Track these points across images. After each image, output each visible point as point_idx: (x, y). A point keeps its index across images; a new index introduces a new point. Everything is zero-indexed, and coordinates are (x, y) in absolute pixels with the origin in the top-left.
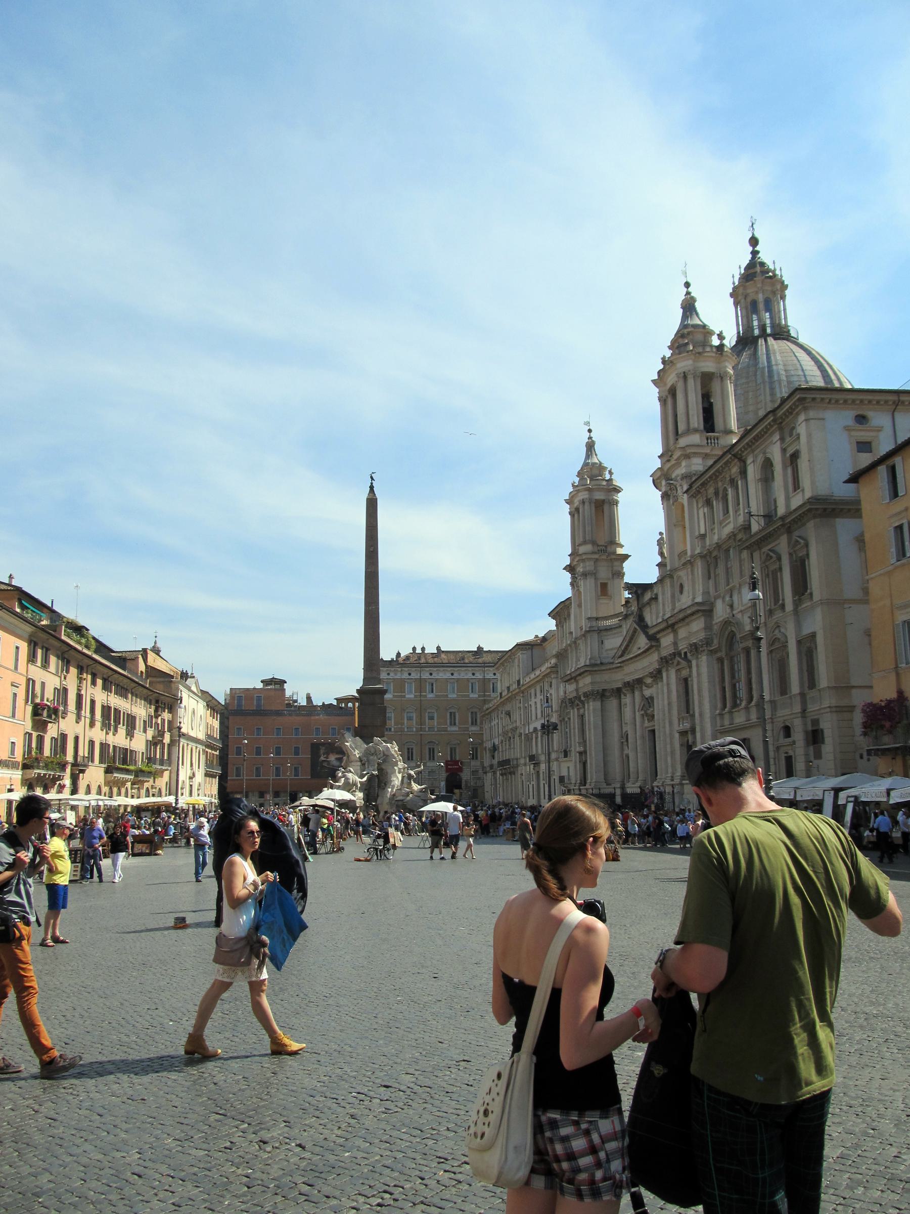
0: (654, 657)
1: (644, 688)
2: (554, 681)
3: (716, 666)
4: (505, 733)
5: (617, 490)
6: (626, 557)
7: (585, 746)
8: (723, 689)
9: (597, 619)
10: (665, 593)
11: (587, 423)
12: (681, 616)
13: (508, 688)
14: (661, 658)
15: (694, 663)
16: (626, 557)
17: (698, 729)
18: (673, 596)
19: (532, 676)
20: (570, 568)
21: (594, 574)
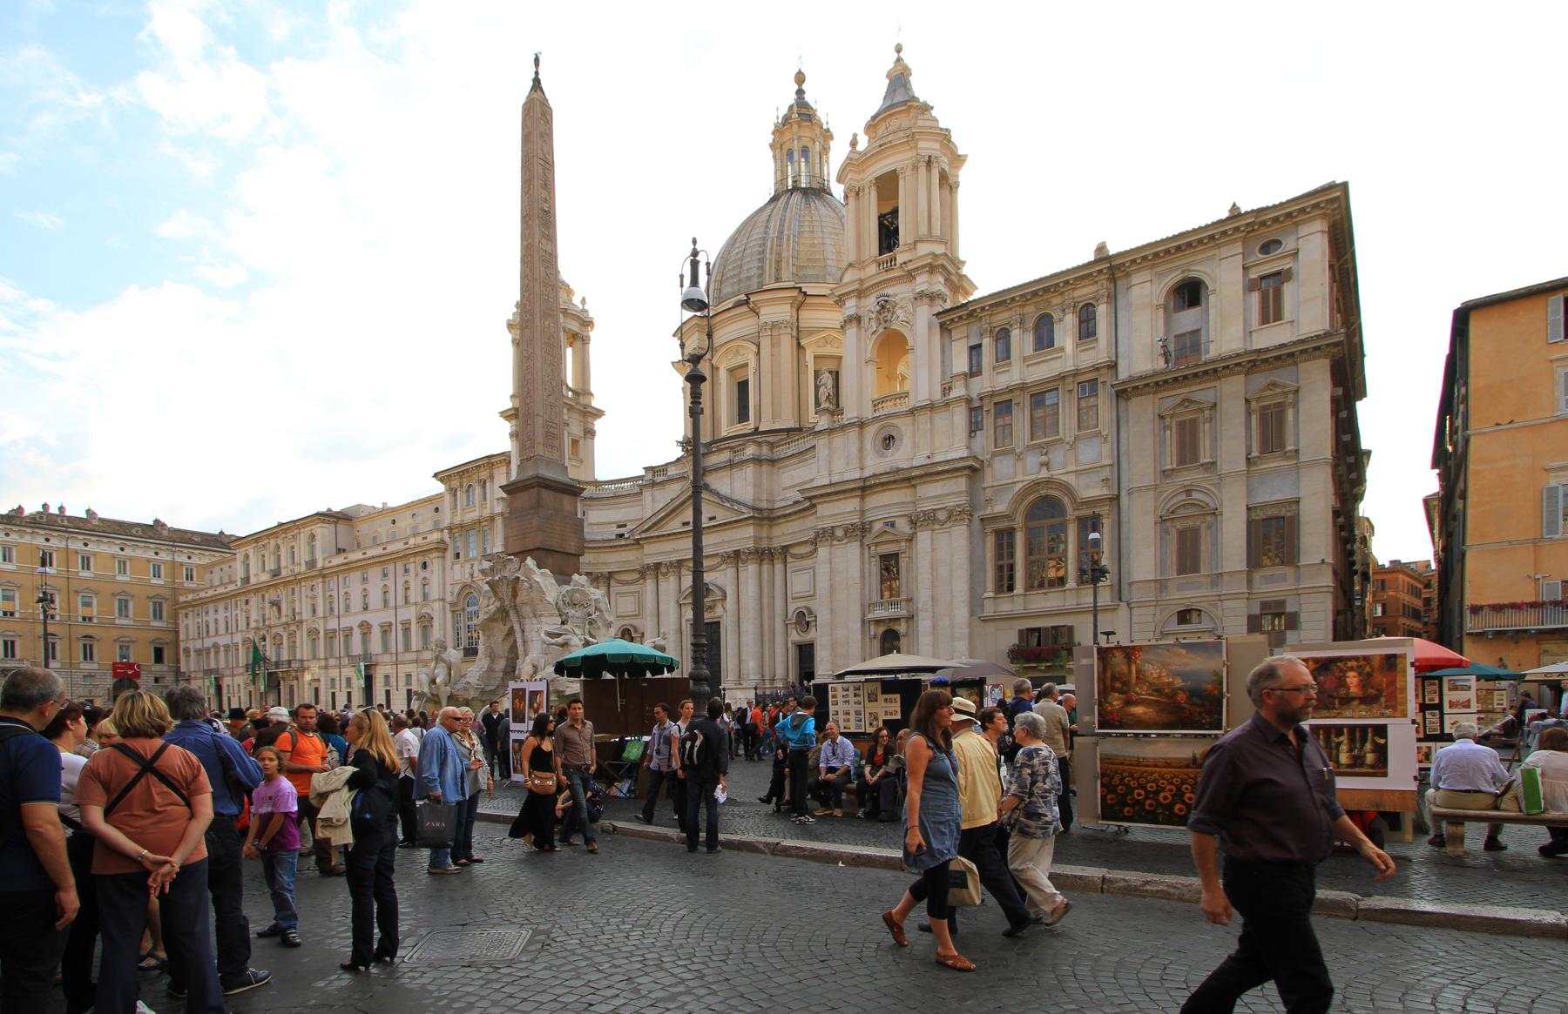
16: (599, 414)
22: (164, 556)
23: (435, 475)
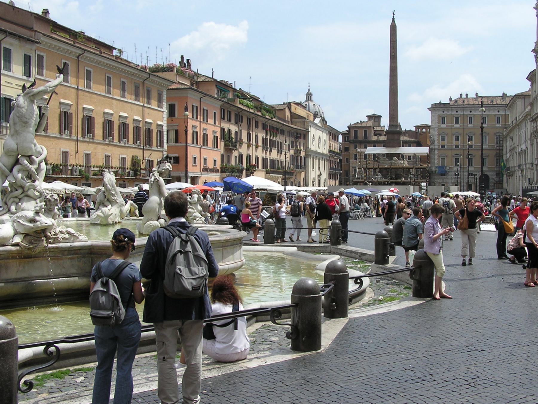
4: (511, 150)
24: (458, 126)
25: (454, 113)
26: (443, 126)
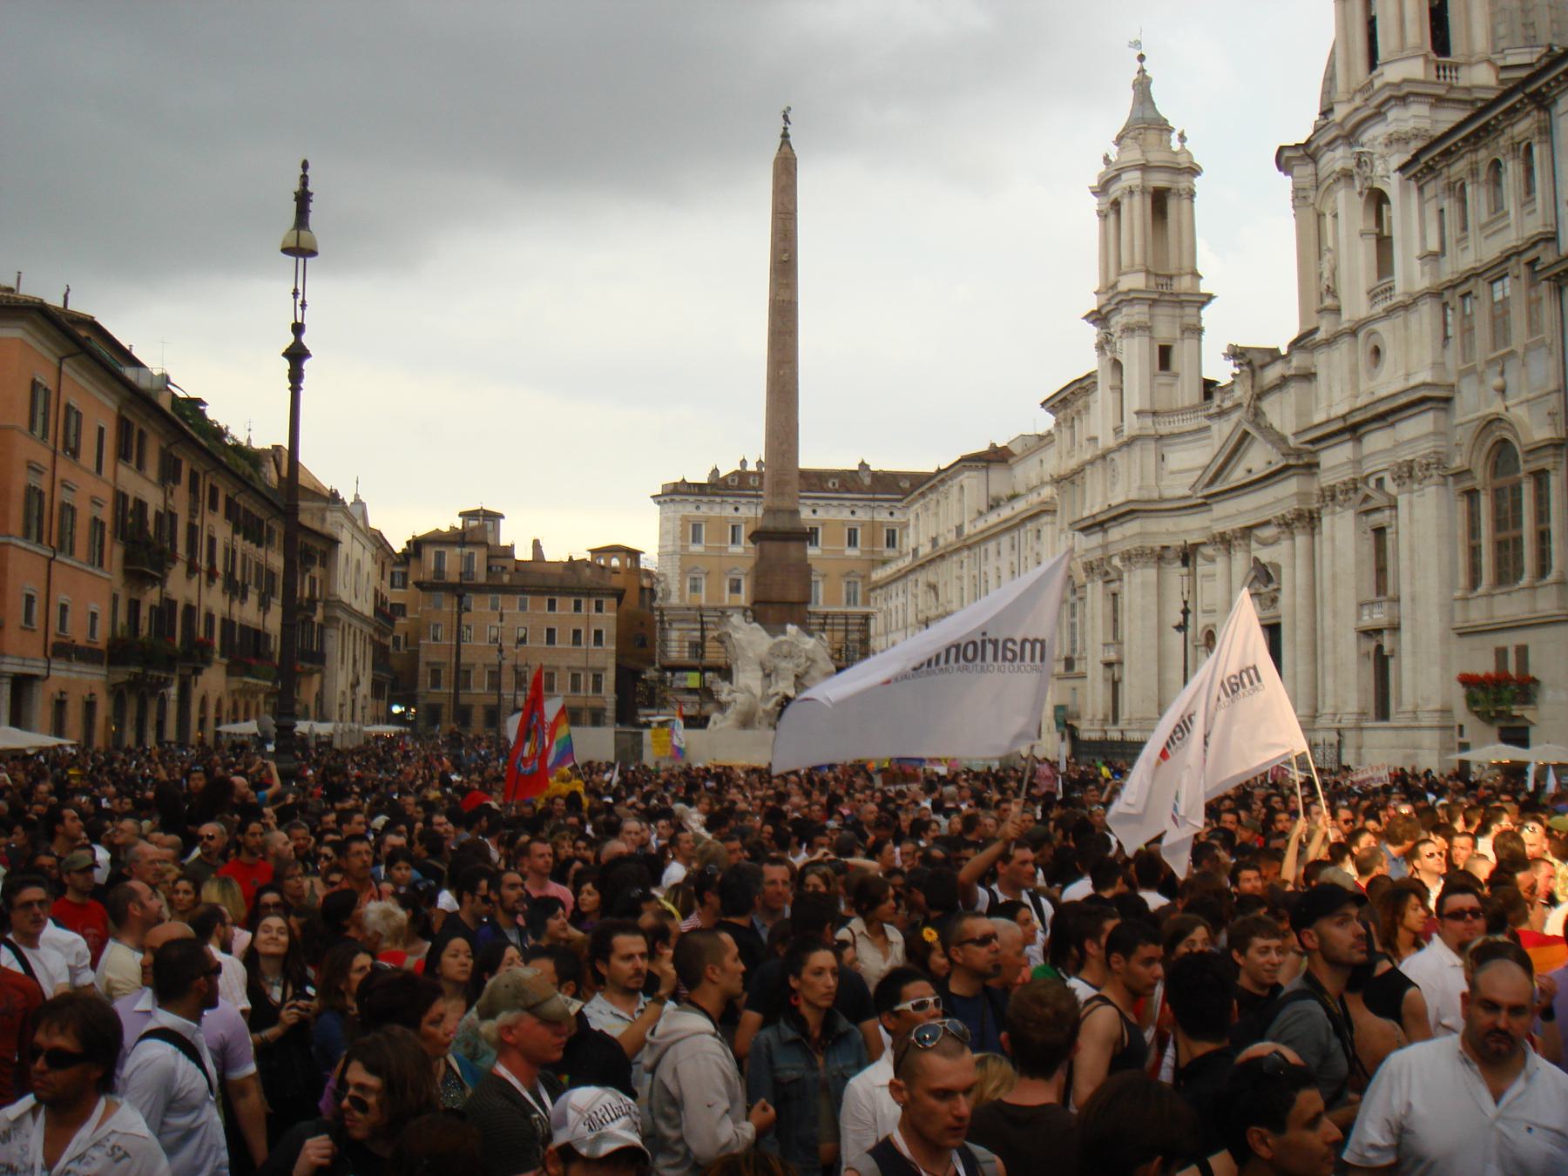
0: (1290, 486)
1: (1254, 545)
2: (1047, 532)
3: (1462, 505)
5: (1194, 171)
6: (1210, 297)
7: (1119, 652)
8: (1474, 552)
9: (1155, 413)
10: (1333, 366)
11: (1137, 44)
12: (1382, 408)
13: (934, 541)
14: (1322, 490)
15: (1403, 501)
16: (1210, 297)
17: (1405, 625)
18: (1354, 371)
19: (993, 518)
20: (1099, 318)
21: (1146, 328)
22: (862, 515)
23: (1043, 405)
24: (737, 550)
25: (728, 511)
26: (696, 548)
